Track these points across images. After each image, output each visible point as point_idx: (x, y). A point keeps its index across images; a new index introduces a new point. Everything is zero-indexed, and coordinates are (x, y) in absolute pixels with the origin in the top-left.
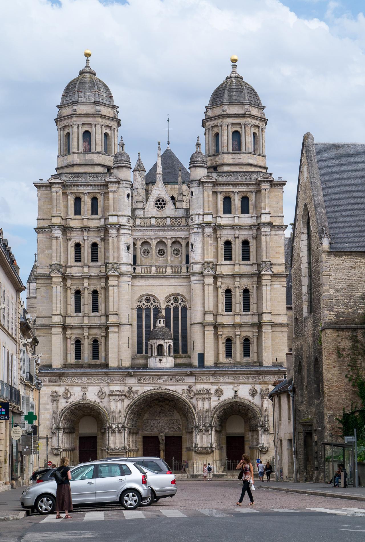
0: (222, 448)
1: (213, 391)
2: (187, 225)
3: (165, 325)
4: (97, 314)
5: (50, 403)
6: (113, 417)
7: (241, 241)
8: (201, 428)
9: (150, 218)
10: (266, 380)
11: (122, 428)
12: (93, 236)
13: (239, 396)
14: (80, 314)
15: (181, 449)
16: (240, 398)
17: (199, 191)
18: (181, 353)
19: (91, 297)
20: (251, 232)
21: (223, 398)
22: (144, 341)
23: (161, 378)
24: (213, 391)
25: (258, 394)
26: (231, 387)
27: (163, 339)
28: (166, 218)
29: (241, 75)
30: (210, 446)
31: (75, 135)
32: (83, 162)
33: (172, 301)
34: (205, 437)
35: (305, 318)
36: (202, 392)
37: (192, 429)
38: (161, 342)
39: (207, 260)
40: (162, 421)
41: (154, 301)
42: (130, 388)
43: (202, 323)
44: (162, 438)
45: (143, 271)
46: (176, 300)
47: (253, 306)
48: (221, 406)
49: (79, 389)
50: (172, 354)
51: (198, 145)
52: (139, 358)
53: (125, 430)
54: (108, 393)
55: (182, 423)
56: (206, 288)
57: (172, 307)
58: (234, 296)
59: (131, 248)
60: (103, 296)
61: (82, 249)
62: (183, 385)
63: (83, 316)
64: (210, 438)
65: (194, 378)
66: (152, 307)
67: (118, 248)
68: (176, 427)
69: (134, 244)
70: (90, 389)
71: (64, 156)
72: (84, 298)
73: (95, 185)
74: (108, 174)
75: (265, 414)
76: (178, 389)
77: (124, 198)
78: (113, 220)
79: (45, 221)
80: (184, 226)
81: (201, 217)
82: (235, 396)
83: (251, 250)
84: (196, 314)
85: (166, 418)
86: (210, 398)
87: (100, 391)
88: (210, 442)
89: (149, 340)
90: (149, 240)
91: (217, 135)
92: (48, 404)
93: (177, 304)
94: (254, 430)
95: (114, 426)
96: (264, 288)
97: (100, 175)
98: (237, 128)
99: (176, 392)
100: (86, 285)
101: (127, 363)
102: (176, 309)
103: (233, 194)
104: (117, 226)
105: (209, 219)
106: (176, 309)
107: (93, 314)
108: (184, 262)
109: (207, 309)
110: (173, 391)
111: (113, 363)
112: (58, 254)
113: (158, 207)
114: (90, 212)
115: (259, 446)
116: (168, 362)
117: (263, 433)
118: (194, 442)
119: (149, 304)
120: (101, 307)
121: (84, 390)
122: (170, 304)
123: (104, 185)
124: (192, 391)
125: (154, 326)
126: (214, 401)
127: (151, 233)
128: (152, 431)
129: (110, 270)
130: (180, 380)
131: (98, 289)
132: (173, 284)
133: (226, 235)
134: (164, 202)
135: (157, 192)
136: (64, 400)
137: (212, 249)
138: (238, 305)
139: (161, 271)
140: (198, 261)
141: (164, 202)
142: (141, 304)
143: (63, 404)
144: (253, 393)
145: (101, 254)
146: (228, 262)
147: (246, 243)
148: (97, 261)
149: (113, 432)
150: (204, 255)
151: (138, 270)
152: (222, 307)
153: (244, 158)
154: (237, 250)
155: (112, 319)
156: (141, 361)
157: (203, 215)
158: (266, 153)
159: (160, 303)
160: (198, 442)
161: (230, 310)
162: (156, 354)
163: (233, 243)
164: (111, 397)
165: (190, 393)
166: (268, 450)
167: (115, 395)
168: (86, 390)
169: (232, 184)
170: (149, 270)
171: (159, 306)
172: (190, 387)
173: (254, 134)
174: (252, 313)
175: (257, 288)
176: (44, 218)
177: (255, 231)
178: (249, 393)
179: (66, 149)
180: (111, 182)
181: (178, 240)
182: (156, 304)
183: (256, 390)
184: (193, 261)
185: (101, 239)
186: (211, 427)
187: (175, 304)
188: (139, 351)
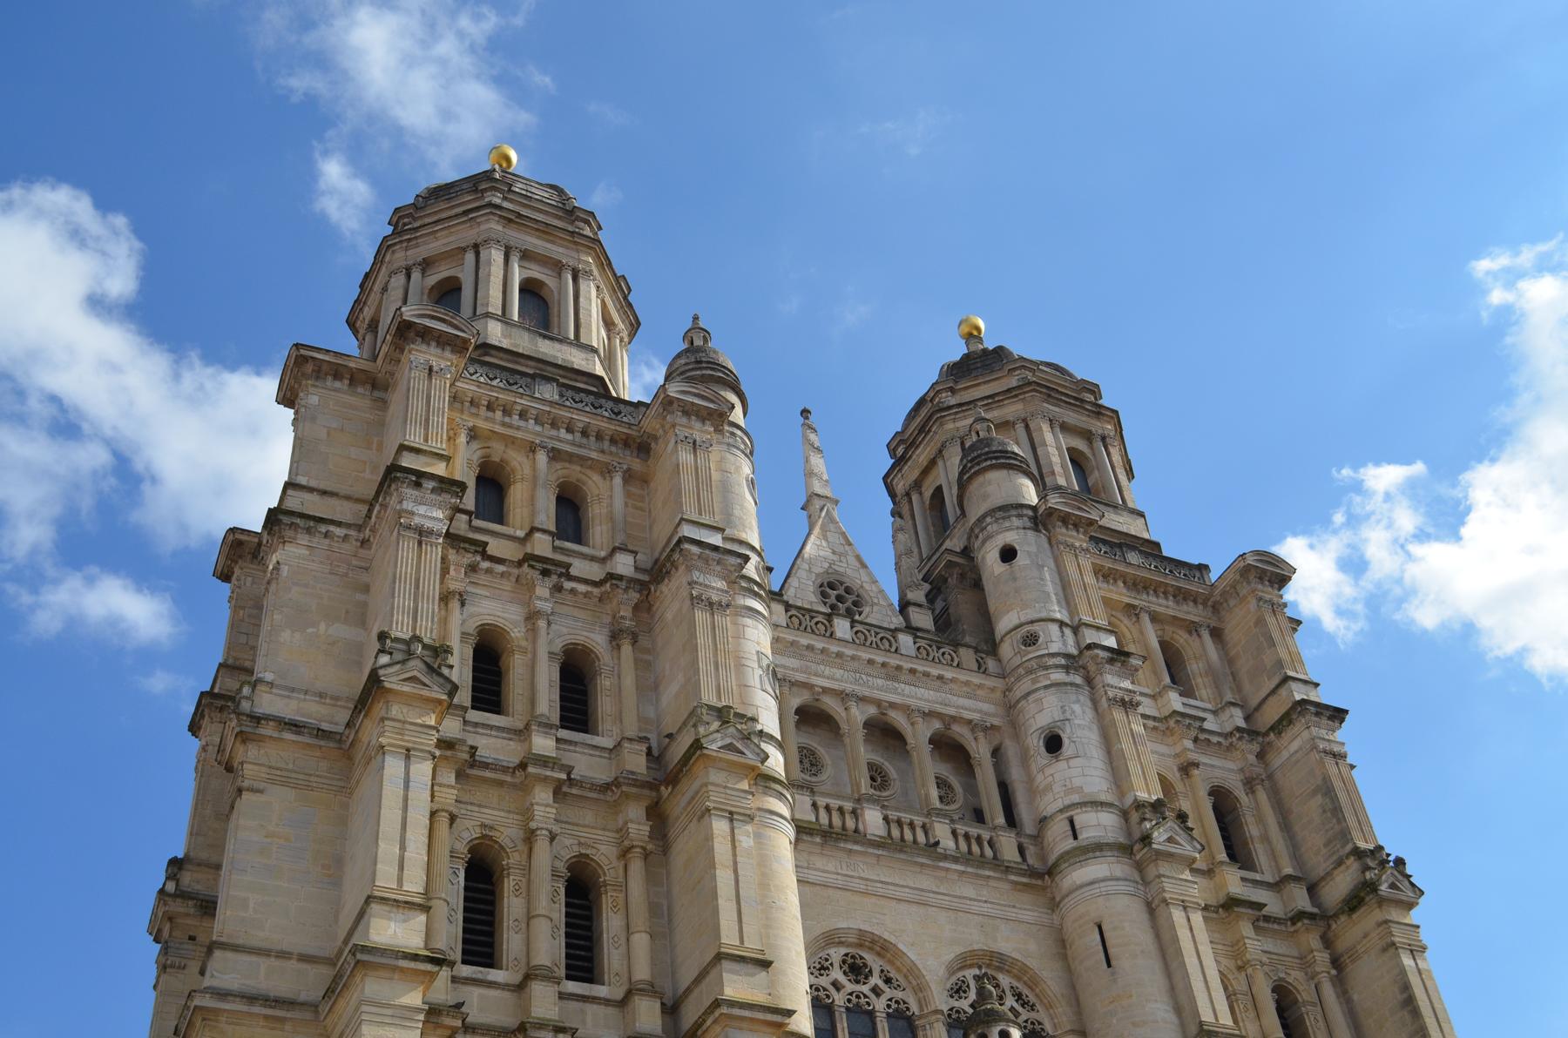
12: (575, 619)
19: (562, 891)
41: (888, 981)
66: (880, 1005)
90: (831, 704)
119: (865, 989)
123: (626, 442)
127: (839, 673)
131: (604, 854)
132: (976, 907)
140: (1103, 798)
159: (920, 989)
171: (914, 1008)
176: (322, 486)
181: (959, 731)
184: (1076, 798)
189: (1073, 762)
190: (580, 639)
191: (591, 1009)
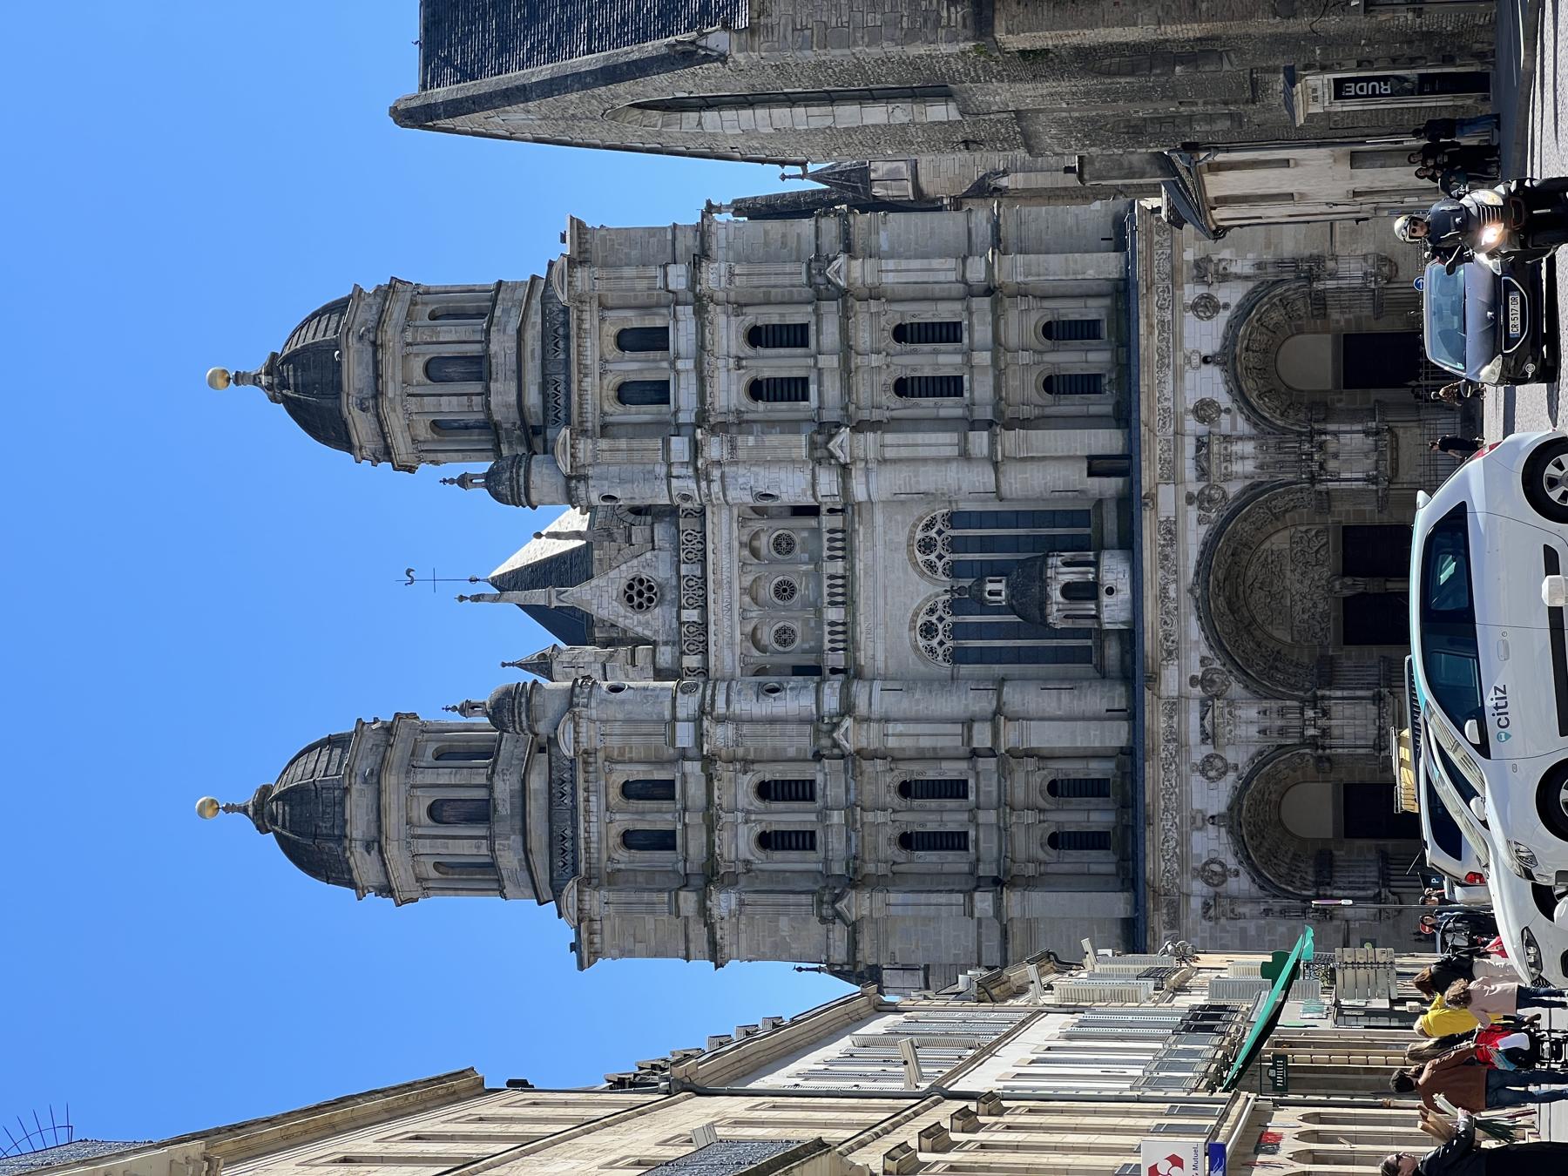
1: (1202, 429)
2: (702, 513)
4: (971, 783)
5: (1241, 923)
6: (1282, 731)
7: (748, 351)
8: (1315, 468)
9: (681, 624)
10: (1168, 268)
11: (1315, 707)
13: (1217, 348)
14: (972, 834)
15: (1381, 527)
17: (600, 478)
18: (1088, 531)
20: (721, 320)
21: (1225, 400)
22: (1054, 643)
23: (1164, 589)
24: (1202, 429)
26: (1189, 375)
28: (679, 577)
29: (265, 359)
30: (1371, 440)
31: (440, 847)
32: (518, 824)
33: (932, 557)
35: (962, 113)
37: (1320, 493)
39: (804, 452)
40: (1298, 586)
42: (1194, 681)
43: (996, 465)
44: (1347, 587)
45: (841, 645)
46: (927, 546)
47: (945, 312)
48: (1247, 403)
49: (1196, 836)
50: (1091, 555)
51: (464, 481)
52: (1102, 657)
53: (1323, 698)
54: (1208, 749)
55: (1302, 524)
56: (890, 453)
57: (948, 557)
58: (914, 370)
59: (772, 681)
60: (916, 767)
61: (774, 828)
62: (1185, 522)
63: (977, 825)
66: (949, 619)
67: (772, 721)
68: (1316, 545)
69: (761, 671)
70: (1196, 805)
71: (500, 881)
72: (923, 825)
73: (586, 790)
74: (553, 750)
75: (1270, 270)
76: (1193, 536)
77: (623, 702)
78: (685, 736)
79: (691, 936)
80: (704, 525)
81: (675, 472)
82: (1218, 364)
83: (775, 320)
84: (969, 484)
85: (1288, 574)
86: (1227, 438)
87: (1203, 773)
89: (1047, 625)
90: (749, 629)
91: (436, 426)
92: (1243, 930)
93: (939, 543)
94: (1320, 302)
95: (1311, 732)
96: (889, 278)
97: (555, 775)
98: (417, 366)
100: (881, 817)
101: (1117, 697)
102: (955, 545)
103: (610, 377)
104: (706, 723)
105: (680, 446)
106: (955, 545)
107: (972, 797)
108: (813, 522)
109: (955, 451)
110: (1202, 553)
111: (1116, 735)
112: (792, 898)
113: (650, 600)
114: (665, 805)
116: (1113, 570)
119: (940, 627)
120: (951, 770)
121: (1199, 823)
122: (940, 564)
123: (586, 763)
124: (1201, 492)
125: (1010, 609)
126: (1234, 427)
129: (836, 745)
130: (1170, 532)
131: (895, 779)
133: (728, 392)
134: (636, 584)
135: (605, 605)
136: (1232, 881)
137: (774, 439)
138: (942, 359)
139: (840, 590)
140: (809, 477)
141: (636, 584)
142: (940, 651)
143: (1241, 884)
144: (1207, 306)
145: (792, 773)
146: (813, 388)
147: (756, 337)
148: (812, 782)
150: (793, 461)
151: (837, 659)
152: (949, 407)
153: (501, 346)
154: (778, 363)
155: (982, 737)
156: (1112, 650)
157: (670, 465)
158: (491, 282)
160: (1360, 475)
161: (958, 380)
163: (753, 374)
165: (1210, 500)
168: (1199, 817)
169: (580, 382)
170: (840, 628)
172: (1190, 499)
173: (433, 317)
174: (965, 314)
175: (889, 301)
177: (719, 309)
179: (482, 875)
180: (576, 742)
181: (745, 539)
182: (940, 606)
183: (1202, 297)
184: (809, 492)
185: (745, 772)
186: (1311, 435)
187: (939, 550)
188: (1081, 656)
189: (784, 489)
190: (752, 792)
191: (982, 788)
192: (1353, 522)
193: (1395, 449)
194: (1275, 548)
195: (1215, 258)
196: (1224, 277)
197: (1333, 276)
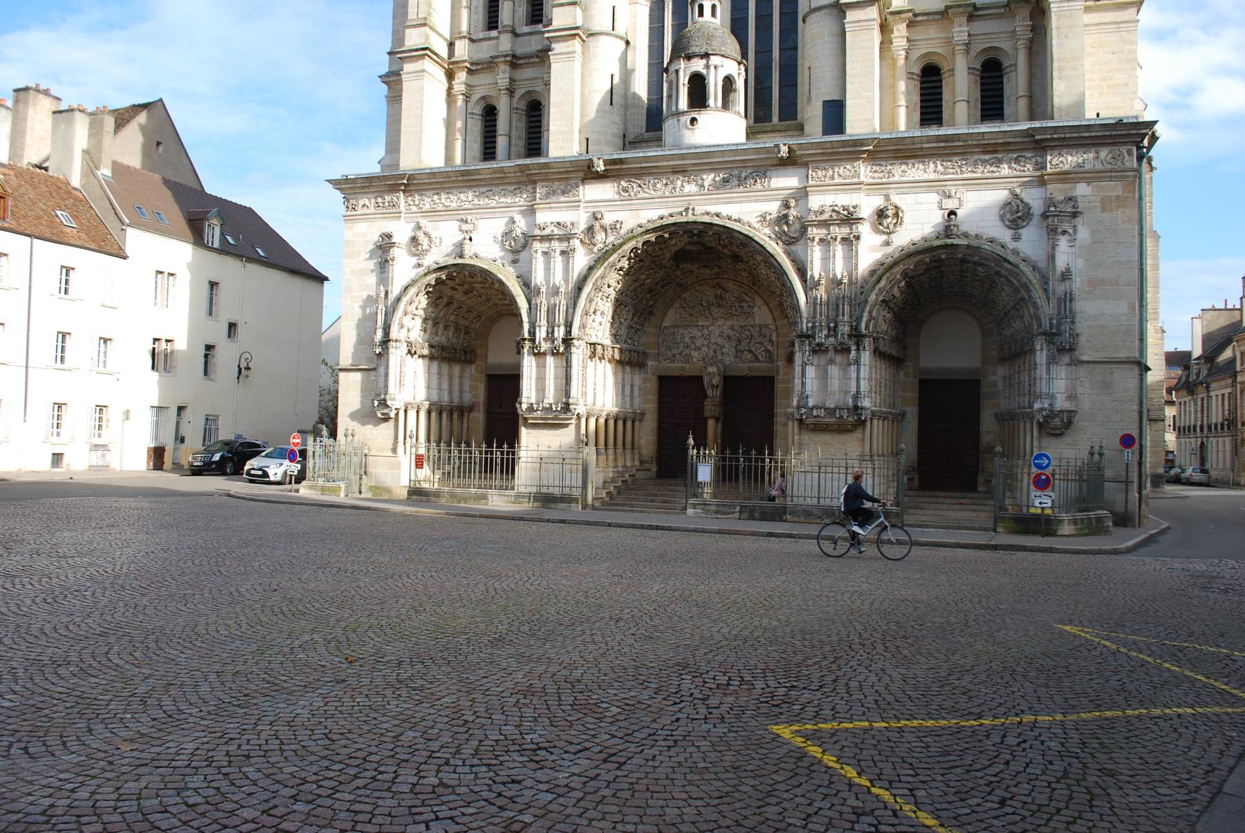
0: (903, 414)
3: (717, 21)
8: (821, 337)
16: (966, 235)
18: (775, 119)
25: (1036, 220)
26: (934, 197)
27: (706, 56)
34: (834, 371)
36: (826, 216)
38: (698, 65)
40: (717, 332)
48: (895, 263)
64: (854, 375)
65: (802, 171)
75: (1060, 289)
76: (748, 211)
82: (947, 228)
86: (858, 238)
88: (854, 389)
99: (739, 221)
107: (526, 29)
115: (1037, 406)
117: (1051, 361)
118: (798, 388)
128: (687, 361)
136: (414, 260)
149: (539, 355)
160: (808, 387)
162: (683, 103)
164: (537, 245)
166: (1070, 423)
167: (548, 238)
178: (1002, 218)
192: (779, 386)
193: (841, 428)
194: (756, 309)
195: (1079, 220)
196: (1053, 232)
197: (1051, 361)
